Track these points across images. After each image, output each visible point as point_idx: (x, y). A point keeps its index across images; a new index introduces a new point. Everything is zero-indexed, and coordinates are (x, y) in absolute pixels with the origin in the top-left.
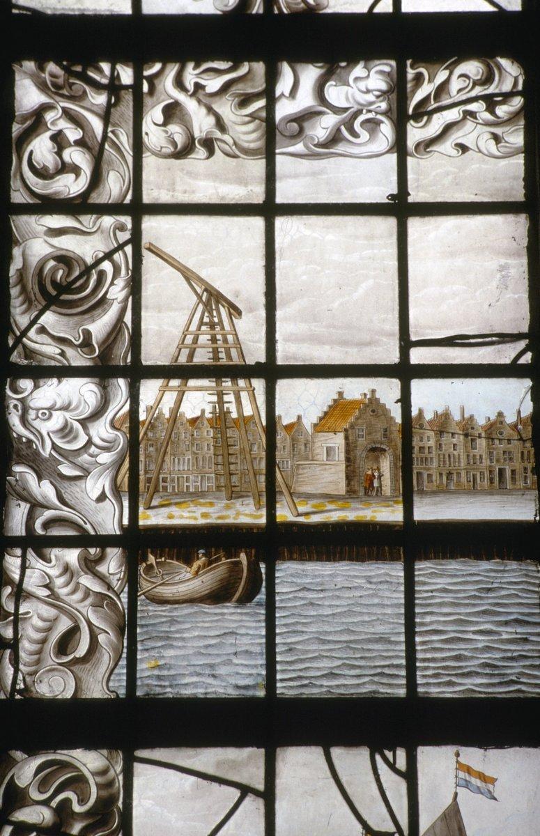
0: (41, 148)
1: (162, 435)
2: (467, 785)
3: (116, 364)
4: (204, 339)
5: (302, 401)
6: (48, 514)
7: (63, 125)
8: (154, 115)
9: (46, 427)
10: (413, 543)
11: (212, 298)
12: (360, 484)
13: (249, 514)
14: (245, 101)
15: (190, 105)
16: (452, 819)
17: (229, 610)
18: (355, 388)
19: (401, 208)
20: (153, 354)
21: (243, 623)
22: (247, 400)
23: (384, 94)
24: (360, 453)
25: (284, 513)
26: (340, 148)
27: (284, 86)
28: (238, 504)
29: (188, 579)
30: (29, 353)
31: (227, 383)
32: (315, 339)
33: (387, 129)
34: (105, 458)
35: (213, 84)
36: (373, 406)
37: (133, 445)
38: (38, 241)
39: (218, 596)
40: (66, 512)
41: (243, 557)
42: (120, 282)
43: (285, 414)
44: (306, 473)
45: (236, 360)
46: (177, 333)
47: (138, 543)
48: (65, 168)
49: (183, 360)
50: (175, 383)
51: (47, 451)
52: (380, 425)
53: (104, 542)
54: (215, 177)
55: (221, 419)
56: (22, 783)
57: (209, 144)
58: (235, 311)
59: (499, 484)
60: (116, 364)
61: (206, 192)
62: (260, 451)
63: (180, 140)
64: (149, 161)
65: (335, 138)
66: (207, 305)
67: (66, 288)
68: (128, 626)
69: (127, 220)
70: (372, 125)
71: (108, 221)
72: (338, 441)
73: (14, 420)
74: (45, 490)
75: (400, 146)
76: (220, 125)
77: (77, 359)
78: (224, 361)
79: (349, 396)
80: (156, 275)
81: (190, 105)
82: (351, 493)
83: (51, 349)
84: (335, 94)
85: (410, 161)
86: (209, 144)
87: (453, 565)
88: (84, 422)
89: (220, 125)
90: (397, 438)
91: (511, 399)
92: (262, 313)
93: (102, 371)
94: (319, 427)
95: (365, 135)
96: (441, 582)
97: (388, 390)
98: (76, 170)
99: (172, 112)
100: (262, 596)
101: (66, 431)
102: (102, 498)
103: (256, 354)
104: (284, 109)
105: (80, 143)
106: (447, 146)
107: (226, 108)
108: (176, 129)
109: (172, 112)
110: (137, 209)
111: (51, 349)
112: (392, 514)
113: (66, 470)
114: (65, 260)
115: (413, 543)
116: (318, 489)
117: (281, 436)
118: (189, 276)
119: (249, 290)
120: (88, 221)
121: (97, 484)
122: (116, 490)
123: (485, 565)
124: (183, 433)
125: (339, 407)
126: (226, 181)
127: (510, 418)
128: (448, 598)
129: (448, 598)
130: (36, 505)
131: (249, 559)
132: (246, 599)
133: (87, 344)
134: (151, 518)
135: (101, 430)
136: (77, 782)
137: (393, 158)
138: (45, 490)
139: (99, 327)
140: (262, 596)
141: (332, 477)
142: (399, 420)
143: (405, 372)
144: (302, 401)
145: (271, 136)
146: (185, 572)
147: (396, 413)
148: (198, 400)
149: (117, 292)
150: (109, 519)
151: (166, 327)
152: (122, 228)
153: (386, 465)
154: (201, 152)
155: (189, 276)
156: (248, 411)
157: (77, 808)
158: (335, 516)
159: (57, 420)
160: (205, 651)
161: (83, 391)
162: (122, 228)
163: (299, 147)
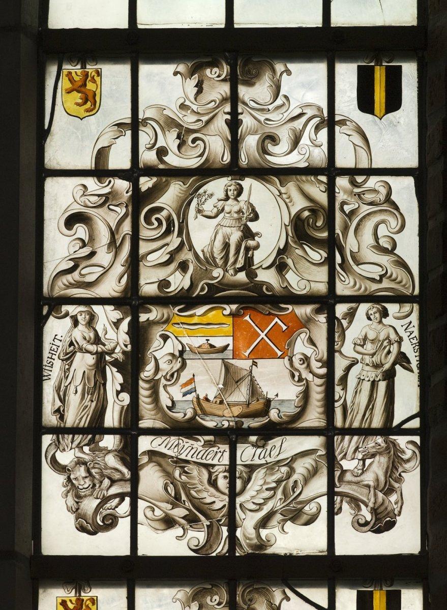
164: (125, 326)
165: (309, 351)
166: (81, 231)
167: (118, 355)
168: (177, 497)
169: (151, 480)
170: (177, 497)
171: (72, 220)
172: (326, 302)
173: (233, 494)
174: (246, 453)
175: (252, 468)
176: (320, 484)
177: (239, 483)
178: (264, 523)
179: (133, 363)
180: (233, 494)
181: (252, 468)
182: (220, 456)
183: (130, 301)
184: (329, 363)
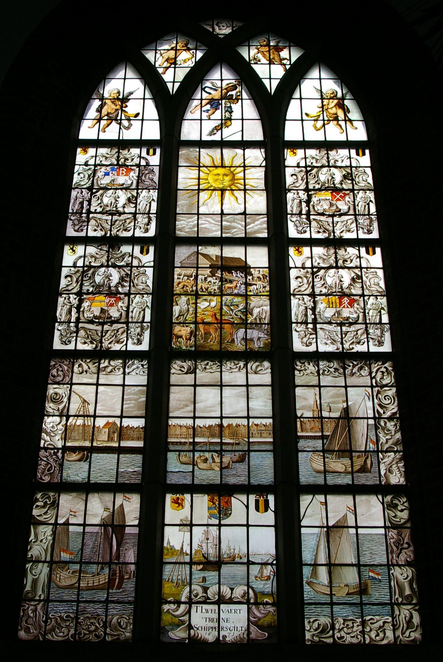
0: (54, 372)
1: (72, 428)
2: (125, 500)
3: (65, 414)
4: (82, 409)
5: (100, 422)
6: (48, 443)
7: (59, 367)
8: (76, 366)
9: (49, 426)
10: (120, 451)
11: (85, 401)
12: (110, 439)
13: (87, 444)
14: (94, 363)
15: (84, 364)
16: (122, 506)
17: (82, 463)
18: (111, 420)
19: (124, 385)
20: (72, 412)
21: (85, 465)
22: (90, 422)
23: (122, 363)
24: (111, 433)
25: (95, 444)
26: (112, 373)
27: (102, 361)
28: (86, 442)
29: (75, 456)
30: (47, 412)
31: (86, 418)
32: (104, 410)
33: (122, 370)
34: (60, 432)
35: (88, 361)
36: (115, 423)
37: (66, 430)
38: (51, 390)
39: (80, 460)
40: (51, 443)
41: (86, 452)
42: (66, 398)
43: (97, 424)
44: (100, 437)
45: (88, 414)
46: (77, 408)
47: (65, 449)
48: (58, 375)
49: (77, 413)
50: (76, 418)
51: (49, 431)
52: (115, 427)
53: (58, 449)
54: (87, 378)
55: (84, 425)
56: (38, 497)
57: (86, 372)
58: (88, 404)
59: (138, 439)
60: (65, 414)
61: (85, 381)
62: (91, 432)
63: (81, 371)
64: (74, 374)
65: (111, 371)
66: (83, 403)
67: (56, 400)
68: (61, 465)
69: (69, 386)
70: (119, 369)
71: (65, 386)
72: (107, 430)
73: (44, 426)
74: (48, 438)
75: (124, 373)
76: (89, 368)
77: (57, 413)
78: (85, 414)
79: (110, 421)
80: (74, 397)
81: (84, 364)
82: (108, 440)
83: (52, 411)
84: (112, 363)
85: (126, 376)
86: (86, 372)
87: (127, 455)
88: (56, 425)
89: (89, 368)
90: (118, 429)
91: (141, 423)
92: (94, 404)
93: (61, 416)
94: (103, 427)
95: (117, 371)
96: (125, 459)
97: (118, 421)
98: (60, 376)
99: (80, 365)
100: (88, 460)
101: (53, 427)
102: (59, 440)
103: (92, 413)
104: (102, 366)
105: (62, 371)
106: (133, 373)
107: (90, 365)
108: (80, 369)
109: (80, 365)
110: (72, 384)
111: (52, 411)
112: (116, 445)
113: (52, 434)
114: (56, 394)
115: (120, 451)
116: (102, 440)
117: (96, 429)
118: (80, 397)
119: (92, 399)
120: (61, 386)
121: (58, 437)
122: (62, 439)
123: (133, 455)
124: (76, 428)
125: (108, 423)
126: (89, 379)
127: (141, 427)
128: (126, 462)
129: (126, 462)
130: (45, 441)
131: (86, 453)
132: (85, 461)
133: (58, 410)
134: (69, 444)
135: (60, 427)
136: (49, 498)
137: (122, 375)
138: (48, 438)
139: (61, 407)
140: (88, 460)
141: (105, 437)
142: (119, 426)
143: (121, 417)
144: (100, 422)
145: (99, 371)
146: (74, 455)
147: (119, 425)
148: (80, 421)
149: (65, 400)
150: (60, 444)
151: (74, 408)
152: (68, 387)
153: (116, 435)
154: (85, 373)
155: (80, 397)
156: (89, 424)
157: (48, 502)
158: (105, 445)
159: (51, 425)
160: (76, 471)
161: (57, 419)
162: (68, 387)
163: (104, 373)
164: (77, 299)
165: (122, 305)
166: (69, 279)
167: (75, 305)
168: (88, 337)
169: (82, 333)
170: (88, 337)
171: (66, 277)
172: (128, 294)
173: (102, 336)
174: (106, 327)
175: (108, 331)
176: (125, 335)
177: (104, 334)
178: (110, 343)
179: (78, 307)
180: (102, 336)
181: (108, 331)
182: (99, 328)
183: (79, 294)
184: (128, 307)
